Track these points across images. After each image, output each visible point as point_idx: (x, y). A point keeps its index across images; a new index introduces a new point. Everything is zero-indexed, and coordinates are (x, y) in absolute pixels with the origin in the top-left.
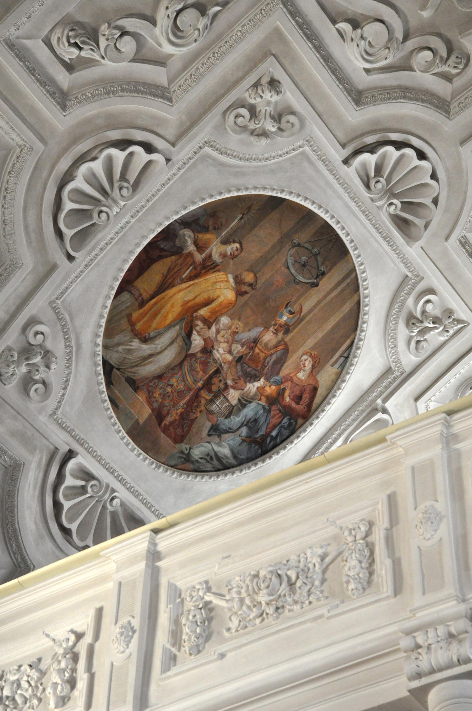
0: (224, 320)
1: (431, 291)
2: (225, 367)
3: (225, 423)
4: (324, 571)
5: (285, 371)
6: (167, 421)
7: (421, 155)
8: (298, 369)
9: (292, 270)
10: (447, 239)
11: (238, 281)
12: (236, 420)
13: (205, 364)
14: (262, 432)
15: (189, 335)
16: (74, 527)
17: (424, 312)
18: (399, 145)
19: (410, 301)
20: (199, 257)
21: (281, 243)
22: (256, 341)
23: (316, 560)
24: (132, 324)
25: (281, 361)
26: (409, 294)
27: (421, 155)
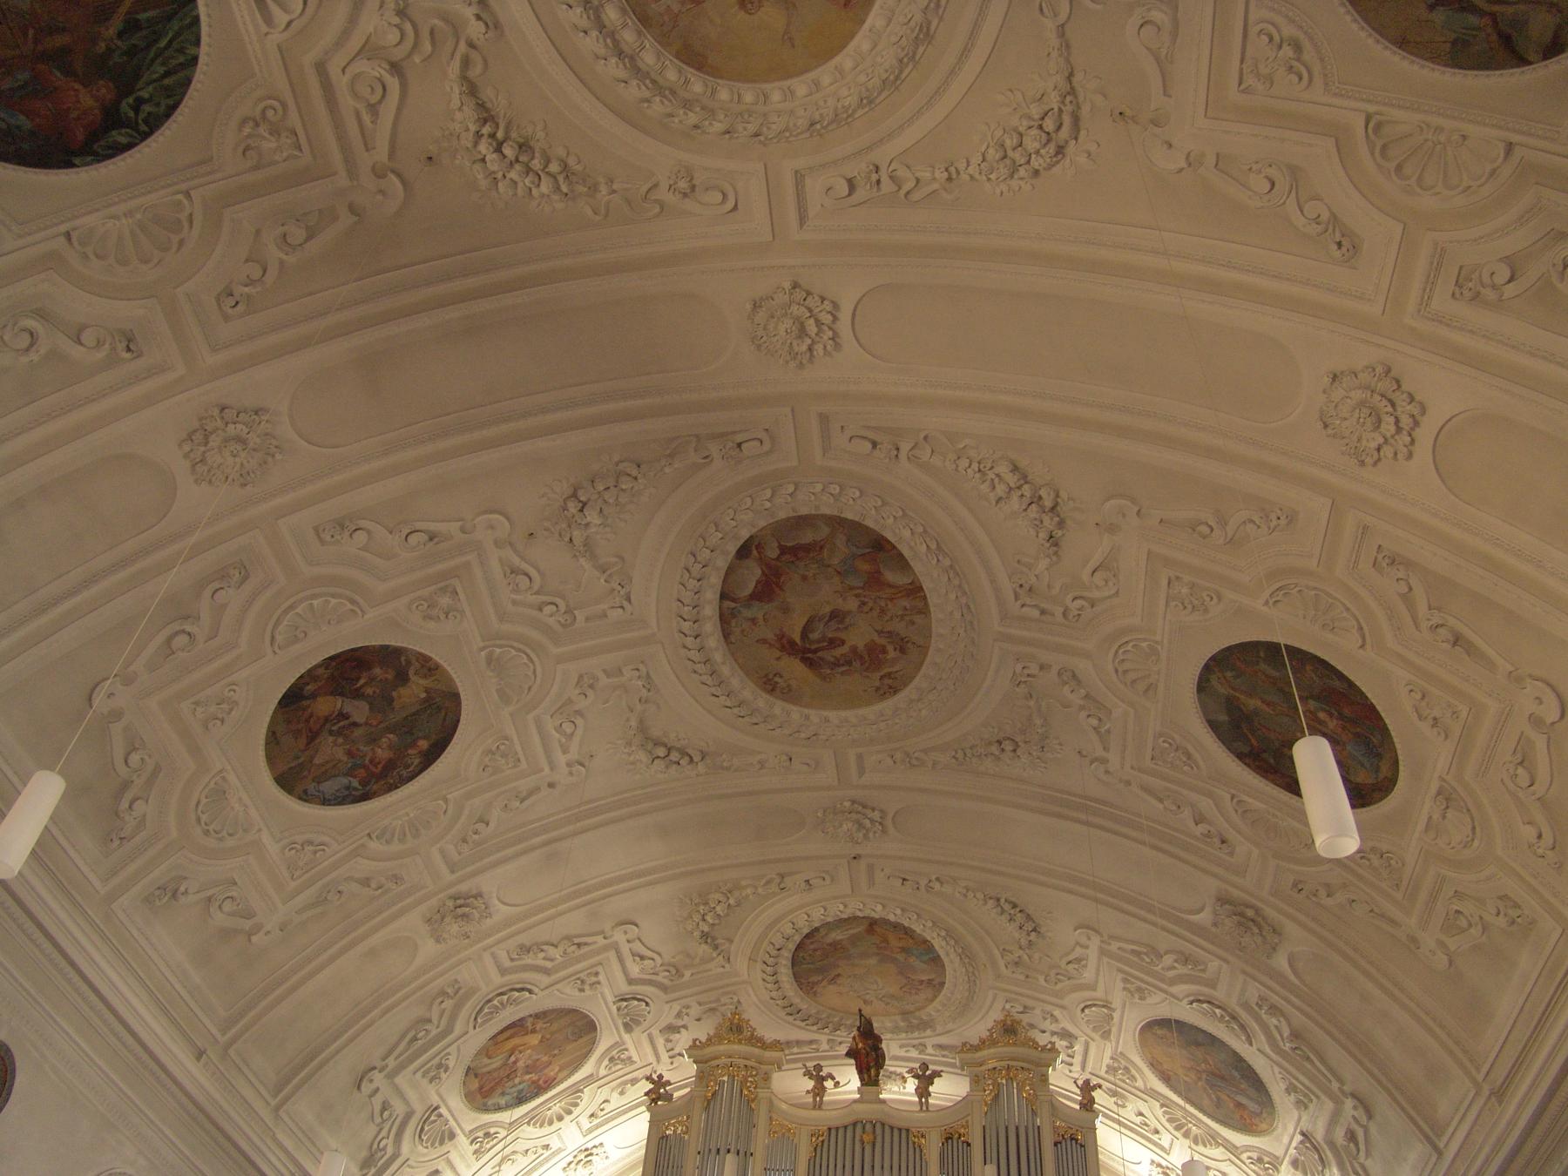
1: (627, 1050)
3: (508, 1091)
7: (647, 1004)
12: (514, 1089)
16: (425, 1138)
18: (639, 1000)
27: (647, 1004)
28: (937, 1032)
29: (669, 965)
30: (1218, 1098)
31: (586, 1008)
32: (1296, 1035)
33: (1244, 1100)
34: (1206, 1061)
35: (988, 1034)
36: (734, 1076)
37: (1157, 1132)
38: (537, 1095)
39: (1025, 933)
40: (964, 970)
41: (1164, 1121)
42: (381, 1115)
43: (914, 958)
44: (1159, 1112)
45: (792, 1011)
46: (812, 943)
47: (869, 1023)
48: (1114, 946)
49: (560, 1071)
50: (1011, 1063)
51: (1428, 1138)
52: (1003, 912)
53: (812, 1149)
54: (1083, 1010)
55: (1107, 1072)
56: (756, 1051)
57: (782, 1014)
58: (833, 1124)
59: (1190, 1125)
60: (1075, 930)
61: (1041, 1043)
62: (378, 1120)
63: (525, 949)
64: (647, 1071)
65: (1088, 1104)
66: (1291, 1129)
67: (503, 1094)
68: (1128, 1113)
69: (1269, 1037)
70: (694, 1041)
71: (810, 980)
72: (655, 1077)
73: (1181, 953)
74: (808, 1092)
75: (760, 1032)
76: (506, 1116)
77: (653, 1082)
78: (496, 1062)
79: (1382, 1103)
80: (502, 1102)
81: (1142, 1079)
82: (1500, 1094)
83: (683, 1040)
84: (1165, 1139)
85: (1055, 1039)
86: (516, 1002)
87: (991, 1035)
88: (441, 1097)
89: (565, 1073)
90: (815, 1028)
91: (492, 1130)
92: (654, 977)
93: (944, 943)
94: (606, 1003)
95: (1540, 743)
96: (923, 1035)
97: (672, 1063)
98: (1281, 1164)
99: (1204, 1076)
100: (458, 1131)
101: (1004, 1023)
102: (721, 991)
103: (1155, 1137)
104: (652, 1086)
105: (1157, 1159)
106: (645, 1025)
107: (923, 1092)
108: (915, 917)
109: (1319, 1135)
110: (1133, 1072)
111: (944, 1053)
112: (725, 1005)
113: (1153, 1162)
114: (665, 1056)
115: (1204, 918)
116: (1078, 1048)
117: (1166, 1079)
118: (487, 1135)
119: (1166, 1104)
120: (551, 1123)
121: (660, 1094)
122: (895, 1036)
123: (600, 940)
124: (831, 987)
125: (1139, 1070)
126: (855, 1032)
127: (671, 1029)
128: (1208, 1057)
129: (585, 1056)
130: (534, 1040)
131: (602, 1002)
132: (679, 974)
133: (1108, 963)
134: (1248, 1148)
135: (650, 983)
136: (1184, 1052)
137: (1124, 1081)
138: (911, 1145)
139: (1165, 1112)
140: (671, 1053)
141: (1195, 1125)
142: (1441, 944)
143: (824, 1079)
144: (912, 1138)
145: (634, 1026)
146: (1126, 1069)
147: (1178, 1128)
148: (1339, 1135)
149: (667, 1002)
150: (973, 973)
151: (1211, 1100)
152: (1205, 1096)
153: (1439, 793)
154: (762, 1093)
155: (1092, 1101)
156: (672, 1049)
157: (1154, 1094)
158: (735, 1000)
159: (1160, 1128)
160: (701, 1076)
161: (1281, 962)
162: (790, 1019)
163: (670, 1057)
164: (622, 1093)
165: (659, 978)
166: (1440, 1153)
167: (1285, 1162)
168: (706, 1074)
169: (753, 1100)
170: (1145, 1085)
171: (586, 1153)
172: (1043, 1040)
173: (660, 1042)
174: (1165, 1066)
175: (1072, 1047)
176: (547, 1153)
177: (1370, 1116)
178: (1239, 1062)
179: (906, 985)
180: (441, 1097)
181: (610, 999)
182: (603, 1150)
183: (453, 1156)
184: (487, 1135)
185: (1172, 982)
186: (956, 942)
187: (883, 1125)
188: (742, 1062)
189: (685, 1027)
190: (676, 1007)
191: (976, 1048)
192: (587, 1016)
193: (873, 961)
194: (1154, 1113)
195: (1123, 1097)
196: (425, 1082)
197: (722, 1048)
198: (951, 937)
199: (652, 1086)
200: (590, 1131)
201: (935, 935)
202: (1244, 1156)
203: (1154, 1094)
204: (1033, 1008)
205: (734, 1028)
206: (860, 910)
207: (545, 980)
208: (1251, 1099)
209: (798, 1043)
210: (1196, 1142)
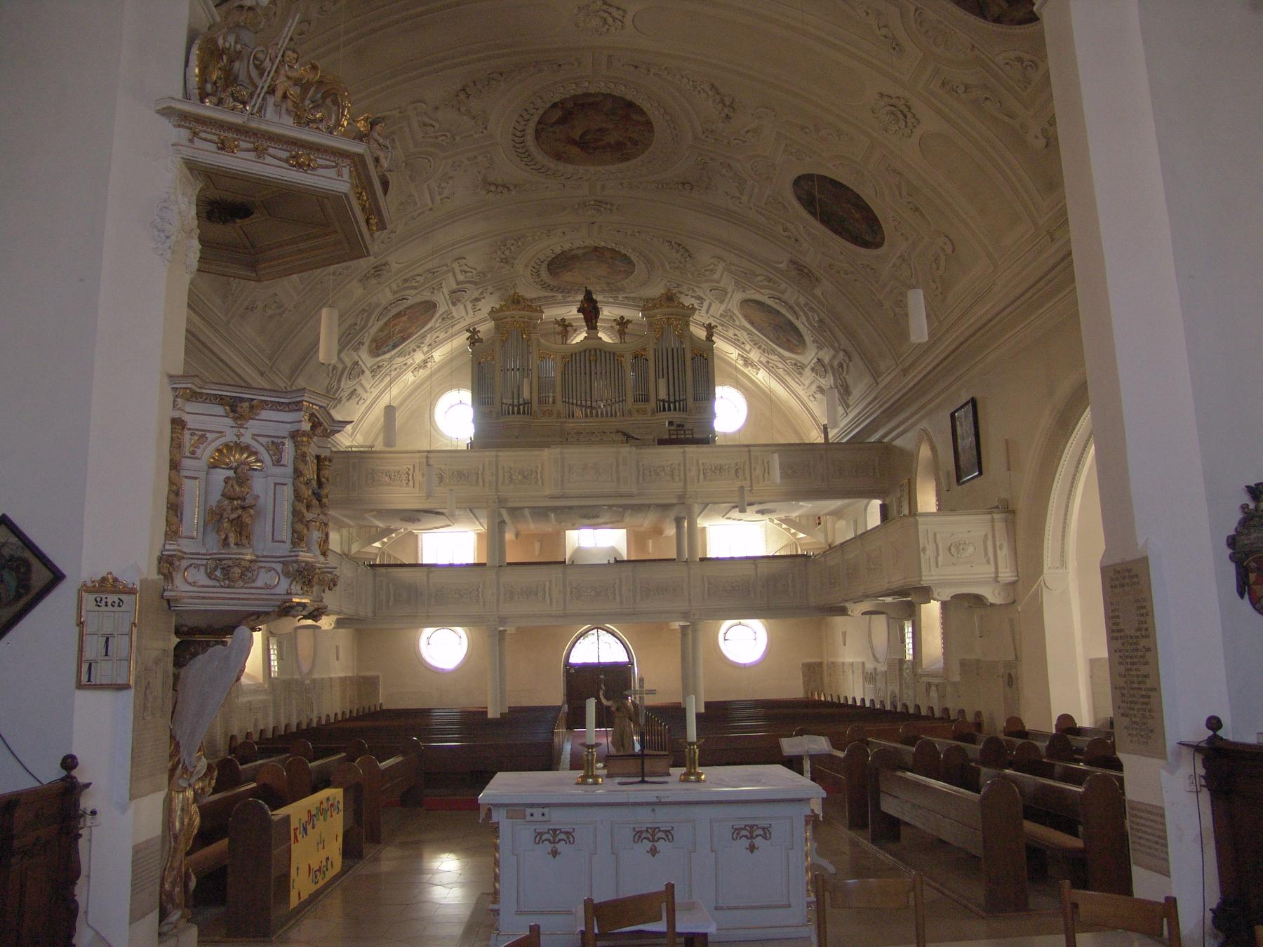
29: (479, 273)
32: (821, 321)
33: (790, 338)
37: (743, 343)
38: (403, 342)
41: (748, 340)
42: (333, 373)
44: (746, 337)
45: (545, 286)
51: (874, 378)
52: (673, 248)
54: (711, 290)
61: (686, 305)
62: (331, 375)
63: (406, 281)
65: (709, 337)
66: (813, 354)
67: (387, 346)
69: (808, 319)
70: (492, 308)
76: (388, 356)
78: (384, 333)
79: (856, 358)
80: (386, 349)
82: (905, 372)
84: (748, 347)
88: (359, 356)
89: (418, 329)
91: (380, 364)
95: (943, 258)
98: (806, 368)
100: (365, 369)
101: (666, 294)
103: (743, 346)
104: (470, 334)
109: (826, 361)
110: (735, 318)
114: (471, 312)
115: (783, 266)
116: (706, 305)
117: (752, 323)
118: (379, 367)
119: (750, 333)
121: (475, 339)
123: (445, 268)
124: (569, 273)
125: (738, 317)
129: (430, 319)
130: (405, 318)
134: (790, 358)
138: (616, 362)
142: (892, 308)
144: (616, 357)
146: (730, 316)
148: (836, 363)
153: (900, 256)
159: (745, 342)
160: (497, 328)
161: (818, 292)
164: (446, 332)
166: (877, 383)
167: (809, 367)
173: (469, 306)
177: (850, 360)
178: (791, 323)
180: (359, 356)
181: (446, 292)
183: (364, 382)
184: (379, 367)
189: (484, 298)
194: (743, 336)
195: (725, 326)
196: (353, 352)
197: (508, 313)
199: (470, 334)
200: (427, 352)
202: (788, 361)
203: (745, 329)
207: (414, 292)
208: (794, 339)
209: (545, 297)
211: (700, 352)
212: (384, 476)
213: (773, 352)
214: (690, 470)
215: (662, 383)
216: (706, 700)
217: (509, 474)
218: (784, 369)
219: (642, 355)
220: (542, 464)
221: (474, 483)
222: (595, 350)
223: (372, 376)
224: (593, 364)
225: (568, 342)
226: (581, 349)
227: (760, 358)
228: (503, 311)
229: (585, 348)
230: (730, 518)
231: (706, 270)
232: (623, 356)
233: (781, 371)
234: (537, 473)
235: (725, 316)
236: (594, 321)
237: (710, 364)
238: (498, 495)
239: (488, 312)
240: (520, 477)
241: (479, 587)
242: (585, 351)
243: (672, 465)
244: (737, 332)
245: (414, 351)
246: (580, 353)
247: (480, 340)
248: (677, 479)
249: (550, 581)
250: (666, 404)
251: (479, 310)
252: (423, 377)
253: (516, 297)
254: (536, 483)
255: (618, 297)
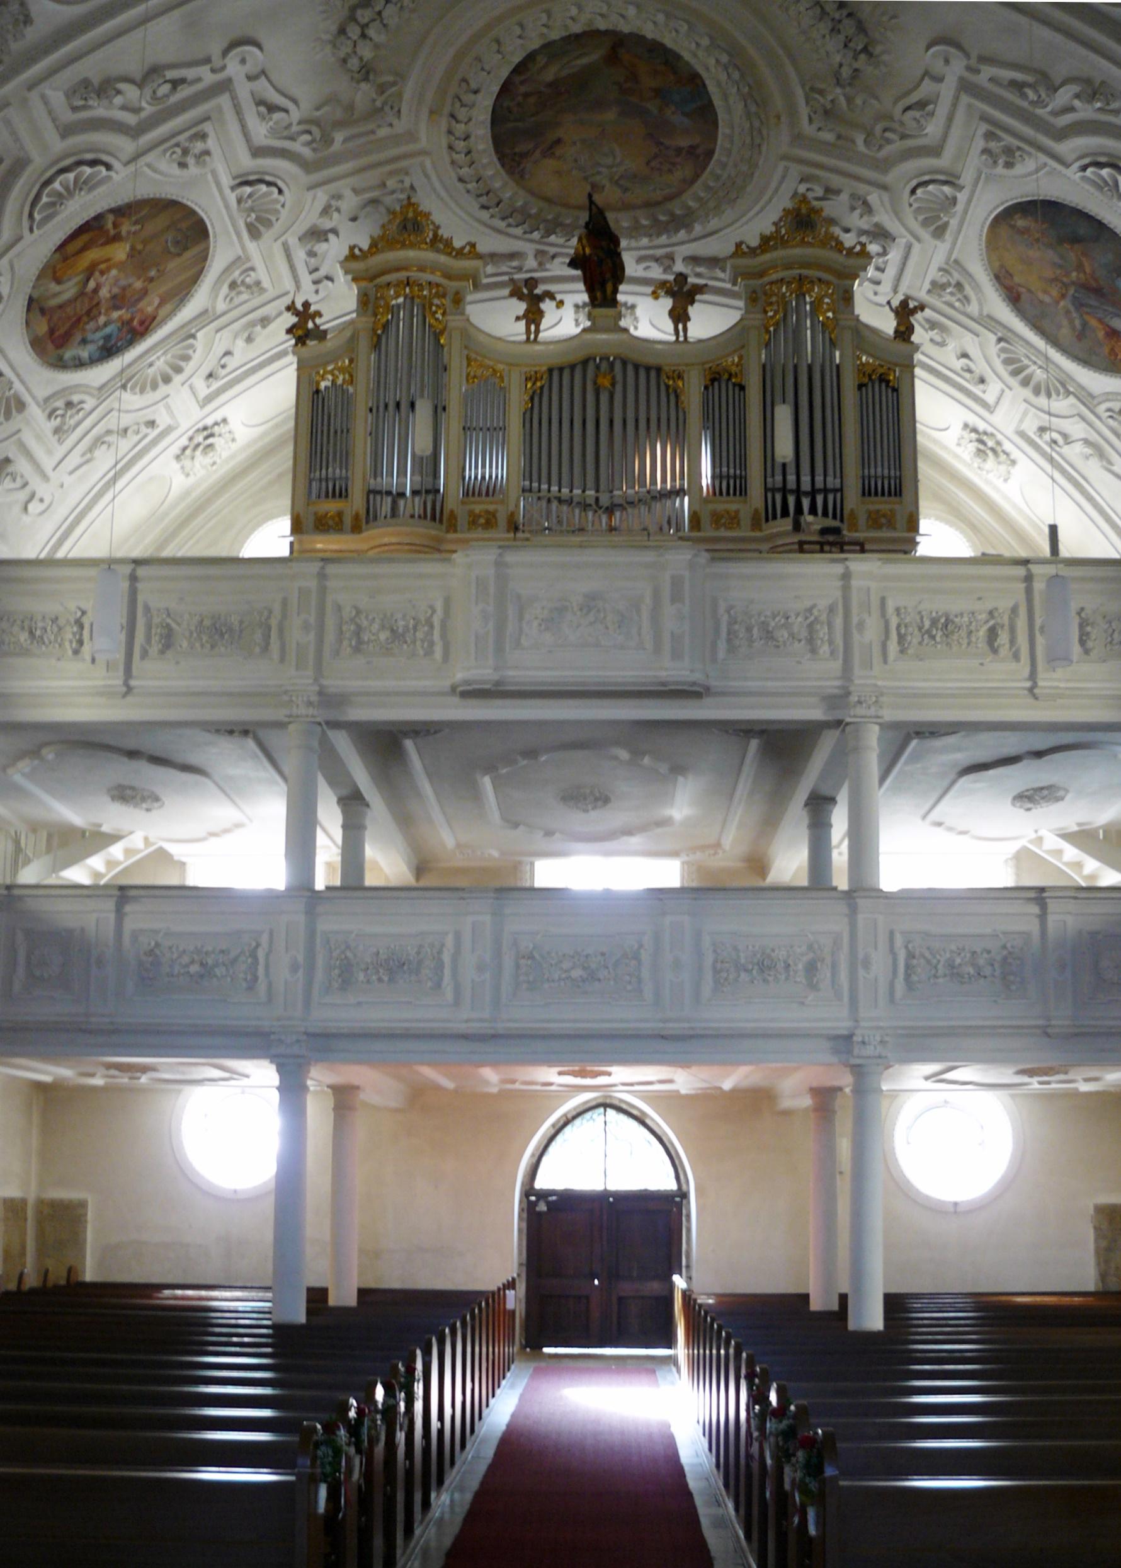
0: (114, 272)
1: (252, 269)
2: (103, 301)
4: (241, 631)
5: (141, 305)
6: (57, 334)
7: (280, 191)
8: (149, 304)
9: (169, 244)
10: (276, 240)
11: (133, 248)
13: (92, 299)
14: (113, 342)
15: (88, 280)
17: (243, 282)
18: (269, 184)
19: (237, 273)
20: (112, 232)
21: (168, 228)
22: (130, 285)
23: (236, 623)
24: (55, 272)
25: (139, 300)
26: (238, 268)
27: (280, 191)
28: (693, 235)
30: (1085, 324)
31: (191, 199)
34: (1080, 267)
35: (773, 229)
36: (412, 298)
37: (982, 381)
39: (851, 54)
40: (748, 125)
43: (673, 108)
44: (993, 349)
45: (488, 199)
46: (522, 83)
47: (601, 212)
48: (988, 71)
49: (160, 306)
50: (805, 272)
53: (527, 398)
54: (913, 192)
55: (929, 291)
56: (443, 259)
57: (473, 205)
58: (556, 361)
59: (1033, 367)
60: (928, 48)
64: (287, 301)
65: (904, 332)
68: (948, 356)
70: (352, 248)
71: (517, 150)
72: (299, 307)
73: (1088, 81)
74: (518, 319)
75: (444, 233)
77: (297, 313)
81: (980, 304)
83: (334, 250)
85: (863, 239)
86: (81, 185)
87: (778, 231)
90: (519, 231)
92: (287, 144)
93: (723, 77)
94: (218, 184)
96: (674, 240)
97: (317, 292)
99: (1071, 291)
102: (388, 168)
103: (976, 390)
104: (295, 319)
105: (973, 420)
106: (278, 227)
107: (679, 316)
108: (686, 27)
110: (968, 290)
111: (699, 270)
112: (393, 192)
113: (966, 426)
114: (306, 279)
116: (894, 256)
117: (1014, 298)
120: (155, 387)
122: (634, 244)
125: (977, 287)
126: (583, 231)
127: (317, 235)
128: (1084, 259)
129: (195, 280)
131: (213, 186)
132: (327, 140)
133: (969, 106)
135: (283, 153)
136: (1050, 255)
137: (952, 306)
139: (1003, 350)
140: (316, 275)
141: (1040, 367)
143: (540, 298)
144: (664, 377)
145: (261, 228)
146: (959, 286)
147: (1015, 373)
149: (310, 188)
150: (760, 132)
151: (1073, 328)
152: (1065, 322)
154: (454, 321)
155: (910, 329)
156: (316, 270)
157: (989, 322)
158: (407, 184)
160: (364, 301)
162: (485, 215)
163: (315, 282)
165: (297, 147)
168: (372, 299)
169: (442, 332)
170: (981, 310)
171: (205, 433)
172: (849, 240)
173: (300, 255)
174: (1017, 279)
175: (884, 253)
176: (153, 433)
179: (656, 156)
181: (226, 181)
182: (227, 428)
185: (1062, 135)
186: (742, 76)
187: (624, 363)
188: (426, 277)
189: (334, 231)
190: (321, 197)
191: (753, 252)
192: (193, 213)
193: (611, 115)
195: (943, 329)
198: (736, 67)
199: (295, 319)
201: (712, 61)
202: (1104, 406)
203: (989, 322)
204: (838, 192)
205: (410, 226)
206: (602, 15)
210: (1037, 392)
211: (881, 371)
212: (16, 629)
213: (1064, 386)
214: (861, 625)
215: (783, 415)
216: (894, 1290)
217: (352, 627)
218: (1086, 442)
219: (730, 375)
220: (447, 602)
221: (257, 650)
222: (612, 365)
223: (57, 431)
224: (604, 398)
225: (542, 336)
226: (571, 358)
227: (1021, 421)
228: (378, 251)
229: (580, 355)
230: (939, 824)
231: (908, 108)
232: (680, 377)
233: (1075, 452)
234: (432, 627)
235: (943, 287)
236: (609, 287)
237: (905, 401)
238: (321, 686)
239: (342, 258)
240: (384, 636)
241: (258, 945)
242: (585, 362)
243: (810, 610)
244: (970, 343)
245: (167, 380)
246: (572, 367)
247: (321, 335)
248: (825, 649)
249: (458, 936)
250: (791, 500)
251: (329, 278)
252: (211, 481)
253: (411, 215)
254: (429, 652)
255: (671, 257)
